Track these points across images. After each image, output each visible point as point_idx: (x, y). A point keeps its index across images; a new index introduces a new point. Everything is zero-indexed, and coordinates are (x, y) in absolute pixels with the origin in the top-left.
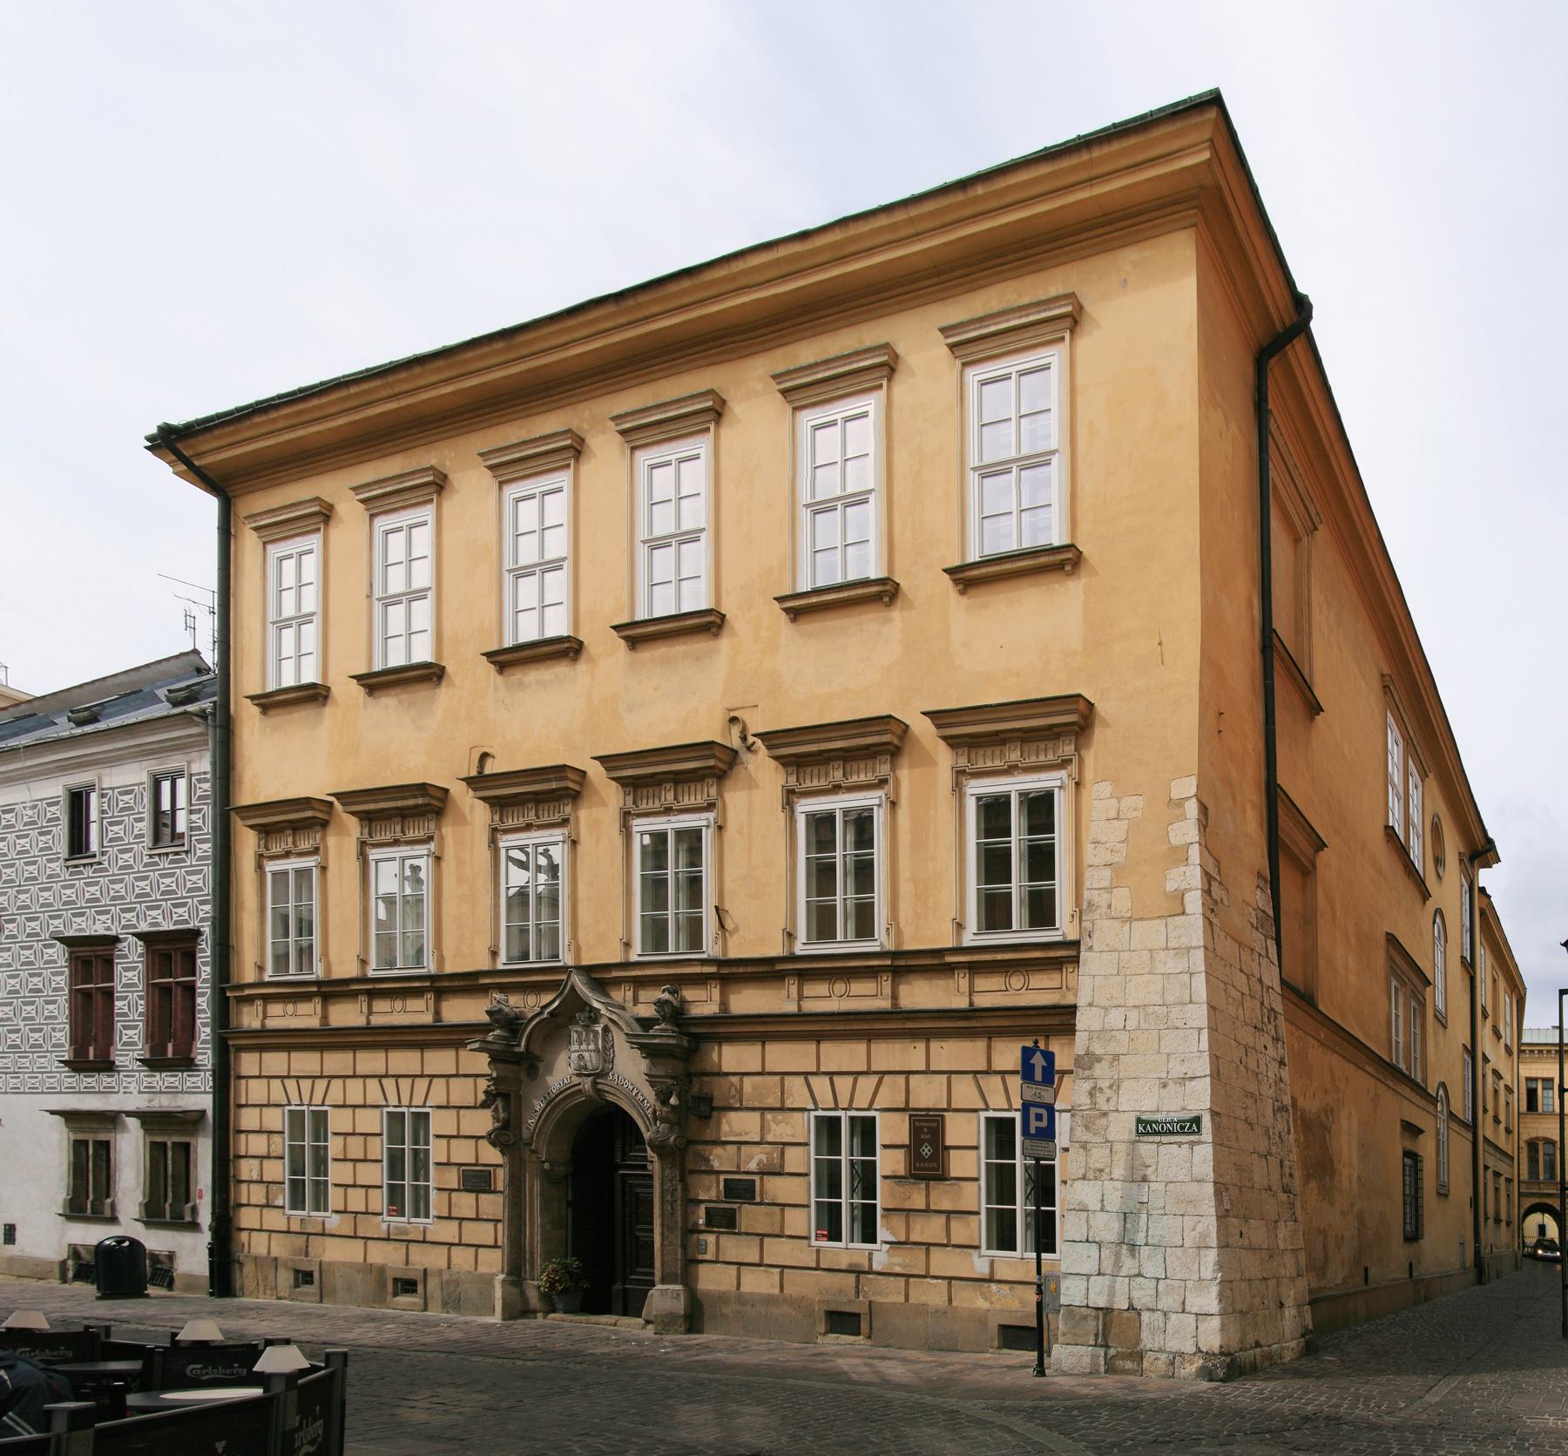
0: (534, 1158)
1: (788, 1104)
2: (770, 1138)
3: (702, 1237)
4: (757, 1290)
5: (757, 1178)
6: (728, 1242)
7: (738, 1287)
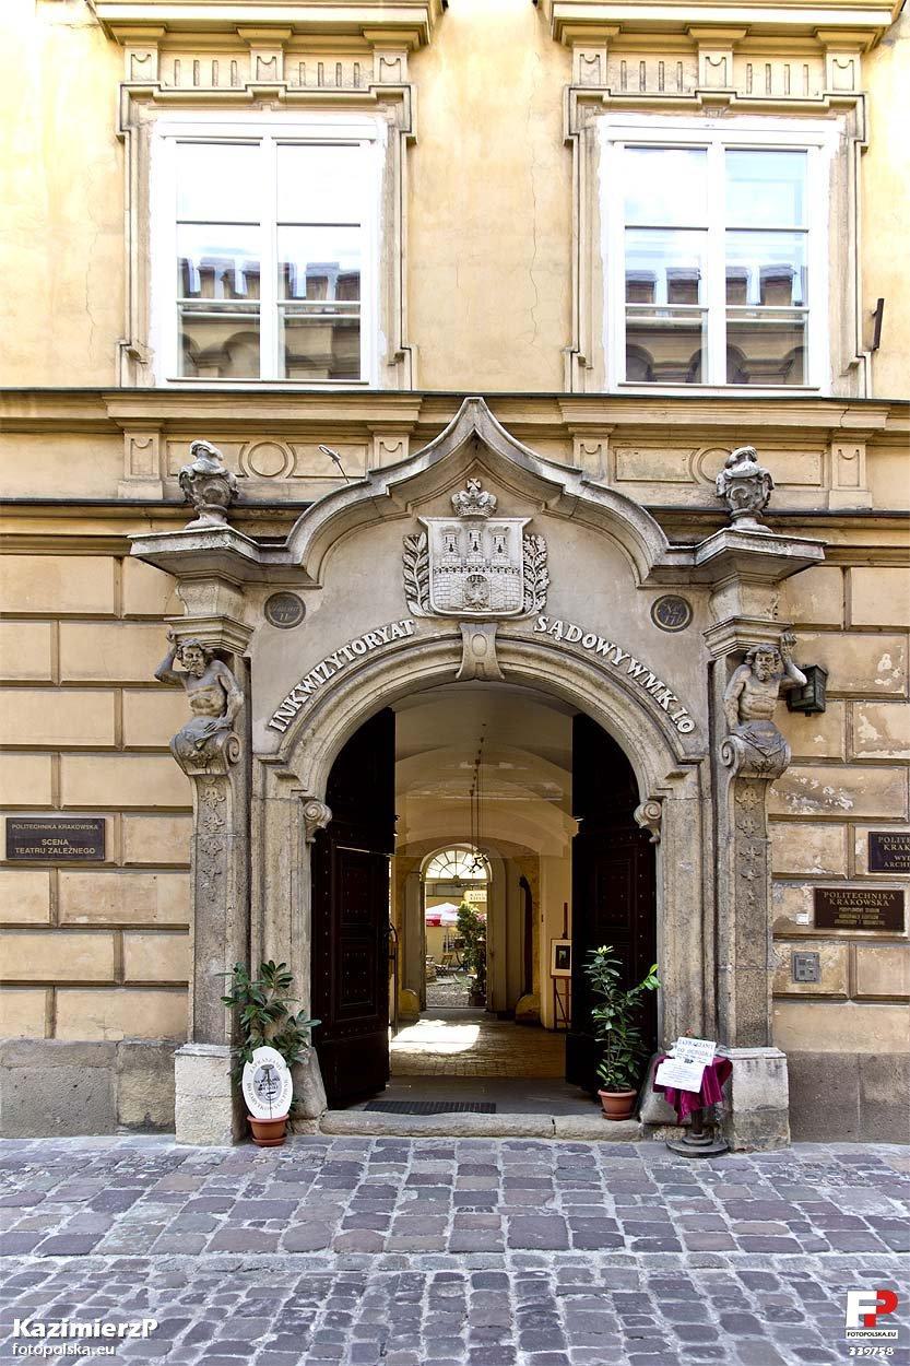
0: (285, 790)
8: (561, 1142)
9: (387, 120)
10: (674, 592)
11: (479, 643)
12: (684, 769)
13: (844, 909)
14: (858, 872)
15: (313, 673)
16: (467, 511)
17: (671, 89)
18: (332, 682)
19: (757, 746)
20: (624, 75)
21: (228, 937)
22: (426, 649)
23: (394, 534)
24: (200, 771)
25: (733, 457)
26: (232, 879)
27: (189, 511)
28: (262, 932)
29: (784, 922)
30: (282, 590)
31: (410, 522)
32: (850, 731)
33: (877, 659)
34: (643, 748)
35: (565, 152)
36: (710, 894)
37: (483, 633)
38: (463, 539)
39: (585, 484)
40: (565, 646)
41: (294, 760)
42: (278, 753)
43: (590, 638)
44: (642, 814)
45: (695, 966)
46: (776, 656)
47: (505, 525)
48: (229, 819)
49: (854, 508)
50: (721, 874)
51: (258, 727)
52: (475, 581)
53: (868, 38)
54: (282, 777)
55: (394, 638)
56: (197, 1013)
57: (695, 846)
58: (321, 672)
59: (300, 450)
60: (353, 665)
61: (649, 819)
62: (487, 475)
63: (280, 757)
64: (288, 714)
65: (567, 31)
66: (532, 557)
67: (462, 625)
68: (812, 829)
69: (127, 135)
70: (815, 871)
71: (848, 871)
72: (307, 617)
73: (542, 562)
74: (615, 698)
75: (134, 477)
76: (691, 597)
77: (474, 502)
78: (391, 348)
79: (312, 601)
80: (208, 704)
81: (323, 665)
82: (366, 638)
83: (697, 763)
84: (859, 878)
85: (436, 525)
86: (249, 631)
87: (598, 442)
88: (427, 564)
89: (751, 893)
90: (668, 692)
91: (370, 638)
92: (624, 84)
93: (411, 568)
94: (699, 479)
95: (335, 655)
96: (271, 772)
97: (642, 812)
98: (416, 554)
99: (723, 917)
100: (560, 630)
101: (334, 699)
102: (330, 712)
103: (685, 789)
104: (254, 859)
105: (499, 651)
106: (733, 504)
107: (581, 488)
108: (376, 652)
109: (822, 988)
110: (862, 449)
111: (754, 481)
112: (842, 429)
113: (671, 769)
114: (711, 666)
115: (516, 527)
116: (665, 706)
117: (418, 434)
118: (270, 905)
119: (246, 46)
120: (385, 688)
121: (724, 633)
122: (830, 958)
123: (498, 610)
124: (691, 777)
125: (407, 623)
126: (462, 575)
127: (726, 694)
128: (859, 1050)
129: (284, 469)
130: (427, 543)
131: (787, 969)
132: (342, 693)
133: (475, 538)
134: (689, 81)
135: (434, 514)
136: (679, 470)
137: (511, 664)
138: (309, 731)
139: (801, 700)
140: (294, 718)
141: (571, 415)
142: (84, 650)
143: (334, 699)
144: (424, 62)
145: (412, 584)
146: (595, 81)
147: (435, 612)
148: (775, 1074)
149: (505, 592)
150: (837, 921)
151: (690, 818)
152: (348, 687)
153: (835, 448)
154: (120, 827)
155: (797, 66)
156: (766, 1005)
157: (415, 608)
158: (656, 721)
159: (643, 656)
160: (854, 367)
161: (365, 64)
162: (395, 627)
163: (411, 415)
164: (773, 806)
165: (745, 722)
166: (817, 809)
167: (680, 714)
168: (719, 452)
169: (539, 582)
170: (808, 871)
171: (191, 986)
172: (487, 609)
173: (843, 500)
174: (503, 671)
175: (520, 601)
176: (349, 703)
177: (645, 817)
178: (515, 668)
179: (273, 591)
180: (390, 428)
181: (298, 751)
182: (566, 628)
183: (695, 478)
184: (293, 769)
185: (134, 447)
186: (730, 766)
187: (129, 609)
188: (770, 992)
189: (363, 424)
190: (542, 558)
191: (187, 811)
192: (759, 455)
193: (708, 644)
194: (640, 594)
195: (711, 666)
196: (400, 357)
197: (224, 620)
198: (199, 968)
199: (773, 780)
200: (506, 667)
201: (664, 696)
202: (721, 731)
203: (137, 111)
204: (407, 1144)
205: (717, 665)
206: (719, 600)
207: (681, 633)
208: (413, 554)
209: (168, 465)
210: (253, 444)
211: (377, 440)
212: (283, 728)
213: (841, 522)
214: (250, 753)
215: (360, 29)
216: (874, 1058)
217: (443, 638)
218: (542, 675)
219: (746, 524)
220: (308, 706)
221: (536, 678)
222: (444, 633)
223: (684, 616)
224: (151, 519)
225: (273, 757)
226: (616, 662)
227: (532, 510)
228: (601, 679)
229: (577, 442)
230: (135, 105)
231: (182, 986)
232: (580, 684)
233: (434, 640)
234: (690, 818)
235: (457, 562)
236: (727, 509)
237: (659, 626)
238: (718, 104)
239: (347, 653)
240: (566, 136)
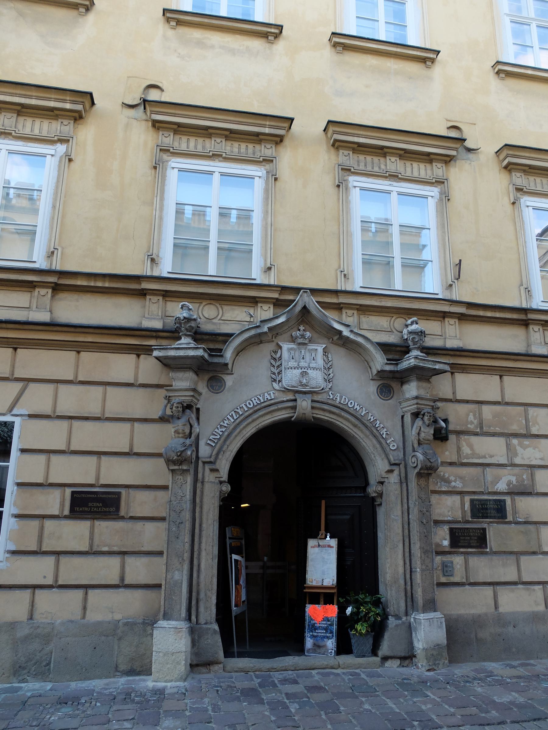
1: (534, 430)
2: (518, 461)
3: (447, 558)
4: (519, 609)
5: (508, 500)
6: (476, 562)
7: (496, 607)
8: (345, 671)
9: (266, 169)
10: (386, 382)
11: (304, 404)
12: (394, 468)
13: (462, 538)
14: (467, 519)
15: (228, 417)
17: (376, 169)
18: (237, 421)
20: (358, 162)
21: (185, 558)
22: (280, 406)
23: (267, 348)
24: (176, 467)
25: (409, 322)
26: (188, 525)
27: (176, 335)
28: (199, 554)
29: (438, 545)
30: (215, 375)
31: (274, 344)
32: (459, 449)
33: (468, 415)
34: (375, 457)
35: (337, 188)
36: (406, 531)
37: (306, 399)
38: (297, 353)
40: (341, 406)
41: (218, 461)
42: (210, 457)
45: (401, 570)
47: (316, 348)
49: (456, 346)
50: (411, 521)
51: (202, 443)
53: (448, 159)
54: (212, 470)
55: (266, 400)
56: (166, 602)
57: (399, 507)
59: (225, 308)
60: (247, 414)
61: (377, 493)
62: (307, 324)
63: (212, 459)
64: (216, 437)
65: (337, 144)
67: (297, 395)
68: (446, 497)
69: (158, 166)
70: (449, 518)
71: (462, 518)
72: (226, 388)
74: (362, 432)
75: (149, 316)
76: (395, 385)
77: (303, 336)
78: (265, 264)
79: (229, 380)
81: (233, 412)
82: (253, 399)
83: (398, 465)
84: (467, 522)
85: (286, 346)
86: (200, 394)
87: (352, 311)
88: (281, 364)
89: (425, 531)
90: (385, 430)
92: (359, 165)
93: (274, 366)
94: (394, 330)
95: (239, 408)
96: (207, 467)
97: (374, 489)
98: (276, 360)
99: (414, 543)
100: (338, 399)
101: (238, 430)
102: (236, 436)
103: (394, 478)
104: (197, 515)
105: (313, 408)
106: (410, 343)
108: (258, 407)
109: (456, 579)
110: (457, 321)
112: (450, 312)
113: (388, 468)
114: (403, 417)
116: (384, 436)
117: (278, 304)
118: (204, 540)
119: (210, 136)
120: (260, 425)
121: (409, 403)
122: (458, 563)
123: (313, 388)
124: (396, 472)
125: (271, 393)
128: (473, 611)
129: (218, 315)
130: (281, 355)
131: (440, 570)
132: (242, 427)
133: (303, 353)
134: (383, 167)
135: (284, 341)
136: (385, 326)
137: (317, 414)
138: (226, 446)
139: (441, 436)
140: (219, 439)
141: (342, 299)
142: (120, 402)
143: (238, 430)
144: (281, 149)
145: (274, 374)
146: (348, 163)
147: (285, 388)
148: (440, 627)
149: (316, 378)
150: (460, 544)
151: (396, 492)
152: (244, 424)
153: (446, 320)
155: (422, 166)
156: (434, 589)
157: (275, 385)
158: (380, 443)
159: (374, 412)
160: (451, 286)
161: (258, 147)
162: (266, 394)
163: (276, 295)
164: (432, 488)
166: (448, 487)
167: (390, 440)
168: (401, 319)
170: (446, 519)
171: (163, 587)
173: (451, 344)
175: (323, 384)
176: (244, 432)
177: (375, 492)
178: (318, 416)
179: (211, 375)
180: (265, 300)
181: (220, 456)
182: (341, 397)
184: (217, 466)
188: (435, 583)
189: (254, 298)
190: (330, 364)
191: (165, 488)
192: (419, 321)
193: (401, 407)
194: (372, 382)
195: (403, 417)
196: (270, 269)
198: (168, 577)
200: (315, 415)
201: (384, 432)
202: (409, 449)
203: (162, 156)
204: (270, 677)
205: (405, 417)
206: (406, 387)
207: (389, 401)
208: (275, 359)
209: (166, 311)
210: (204, 304)
211: (259, 305)
212: (213, 445)
213: (452, 353)
214: (197, 457)
215: (258, 134)
216: (480, 616)
217: (288, 401)
218: (330, 420)
219: (415, 353)
220: (226, 434)
221: (328, 421)
222: (288, 398)
224: (157, 337)
225: (208, 460)
226: (362, 414)
227: (326, 340)
228: (357, 422)
229: (344, 311)
230: (162, 153)
231: (158, 586)
232: (347, 424)
233: (283, 402)
234: (396, 492)
235: (295, 364)
236: (406, 345)
237: (380, 398)
238: (394, 177)
240: (337, 183)
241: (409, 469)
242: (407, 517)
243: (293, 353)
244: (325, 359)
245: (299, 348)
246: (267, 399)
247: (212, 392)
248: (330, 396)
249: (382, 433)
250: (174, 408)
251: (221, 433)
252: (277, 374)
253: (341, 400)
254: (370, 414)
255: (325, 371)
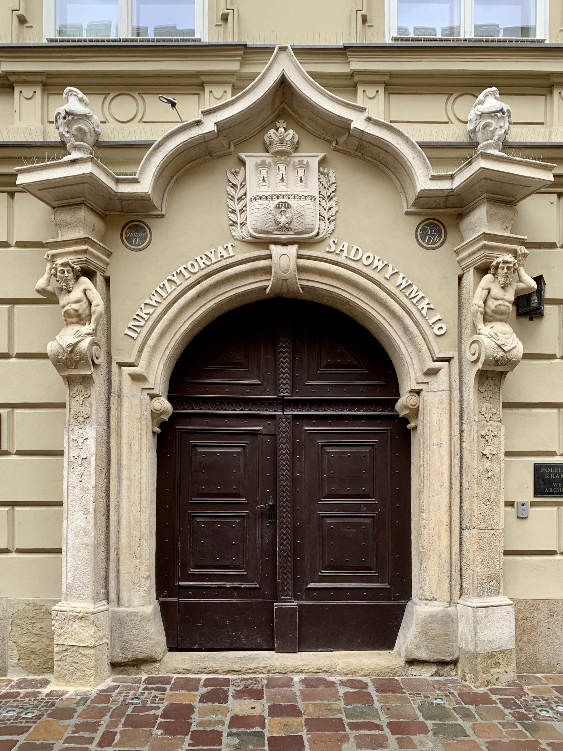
11: (284, 261)
16: (277, 148)
19: (499, 342)
39: (369, 119)
41: (143, 362)
43: (368, 257)
44: (405, 401)
46: (514, 265)
48: (94, 412)
52: (283, 206)
55: (220, 258)
58: (163, 287)
66: (325, 188)
67: (272, 247)
73: (333, 192)
80: (76, 314)
81: (165, 282)
88: (245, 194)
91: (201, 258)
95: (174, 273)
107: (365, 124)
111: (499, 115)
114: (460, 278)
115: (314, 163)
116: (424, 312)
118: (125, 483)
126: (272, 202)
127: (476, 300)
139: (528, 307)
141: (357, 65)
145: (234, 212)
147: (251, 236)
154: (10, 417)
165: (489, 324)
169: (330, 209)
172: (291, 233)
174: (303, 287)
182: (350, 248)
183: (449, 119)
185: (22, 97)
186: (475, 362)
187: (18, 237)
189: (197, 75)
193: (458, 258)
196: (225, 18)
197: (86, 241)
199: (507, 372)
208: (234, 186)
220: (155, 316)
223: (440, 236)
239: (184, 271)
241: (465, 368)
242: (458, 447)
243: (264, 172)
244: (323, 180)
245: (275, 163)
246: (222, 256)
247: (130, 249)
248: (330, 247)
249: (420, 307)
250: (58, 274)
251: (146, 317)
252: (238, 213)
253: (349, 253)
254: (401, 275)
255: (323, 203)
